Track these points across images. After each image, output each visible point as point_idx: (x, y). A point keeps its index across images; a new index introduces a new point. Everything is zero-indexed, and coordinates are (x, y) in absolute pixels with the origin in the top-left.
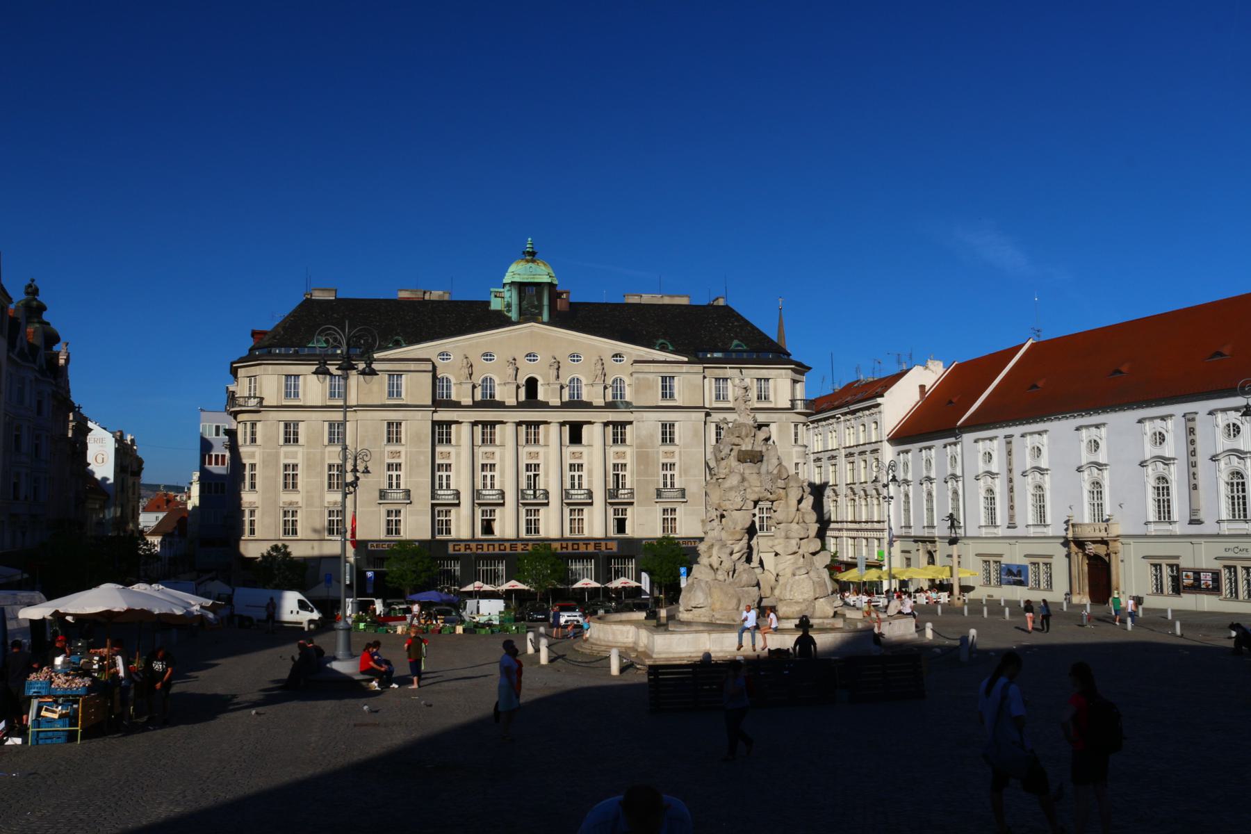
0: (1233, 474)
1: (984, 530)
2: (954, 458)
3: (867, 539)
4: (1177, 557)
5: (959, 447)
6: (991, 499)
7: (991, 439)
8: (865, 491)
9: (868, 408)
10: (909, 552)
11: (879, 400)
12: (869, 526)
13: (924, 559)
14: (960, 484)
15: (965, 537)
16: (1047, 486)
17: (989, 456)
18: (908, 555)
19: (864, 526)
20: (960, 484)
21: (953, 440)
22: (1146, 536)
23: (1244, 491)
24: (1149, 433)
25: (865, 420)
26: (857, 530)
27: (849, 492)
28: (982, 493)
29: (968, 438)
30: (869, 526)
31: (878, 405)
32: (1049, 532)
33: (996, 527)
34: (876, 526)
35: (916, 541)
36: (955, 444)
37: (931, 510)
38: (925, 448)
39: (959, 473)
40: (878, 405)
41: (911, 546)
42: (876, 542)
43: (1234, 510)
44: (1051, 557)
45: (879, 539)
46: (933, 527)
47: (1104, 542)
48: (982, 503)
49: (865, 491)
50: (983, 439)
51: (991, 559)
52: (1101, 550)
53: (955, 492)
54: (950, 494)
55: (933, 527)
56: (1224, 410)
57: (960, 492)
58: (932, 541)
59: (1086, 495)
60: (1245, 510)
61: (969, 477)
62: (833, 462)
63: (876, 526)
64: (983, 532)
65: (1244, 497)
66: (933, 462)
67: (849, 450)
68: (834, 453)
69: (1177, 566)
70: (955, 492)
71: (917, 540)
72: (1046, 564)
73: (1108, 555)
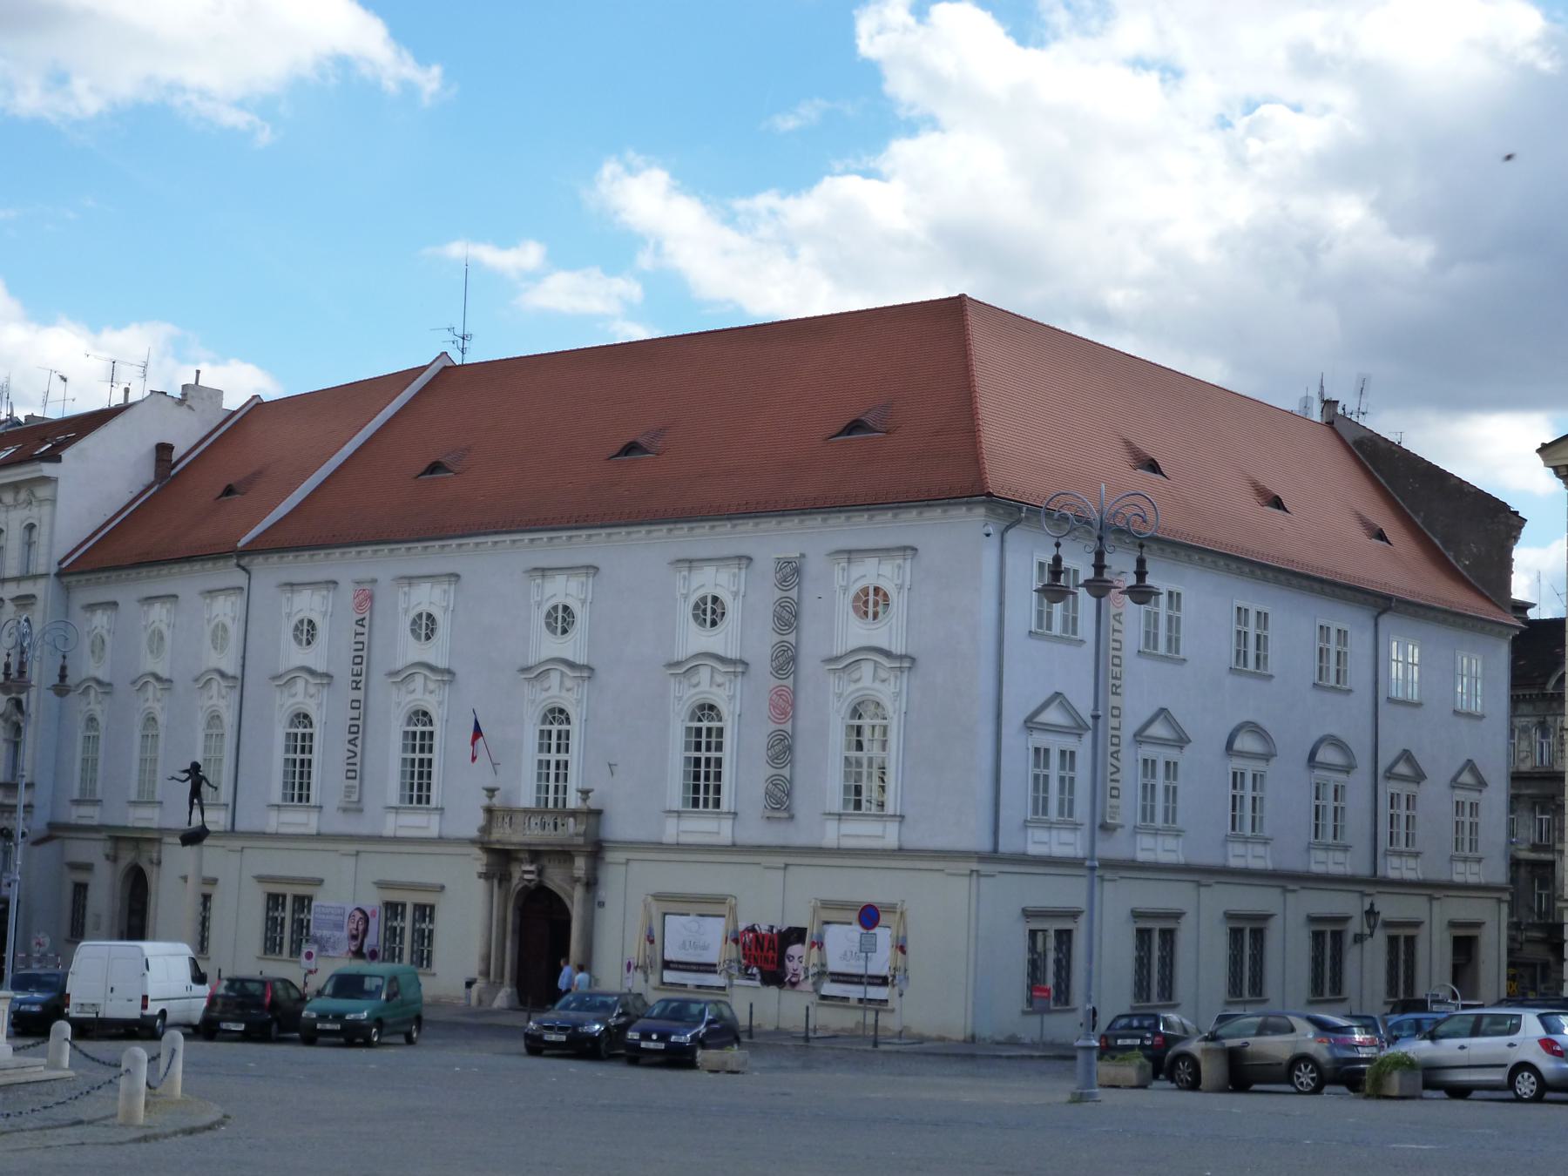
6: (301, 743)
15: (232, 832)
17: (307, 632)
52: (555, 878)
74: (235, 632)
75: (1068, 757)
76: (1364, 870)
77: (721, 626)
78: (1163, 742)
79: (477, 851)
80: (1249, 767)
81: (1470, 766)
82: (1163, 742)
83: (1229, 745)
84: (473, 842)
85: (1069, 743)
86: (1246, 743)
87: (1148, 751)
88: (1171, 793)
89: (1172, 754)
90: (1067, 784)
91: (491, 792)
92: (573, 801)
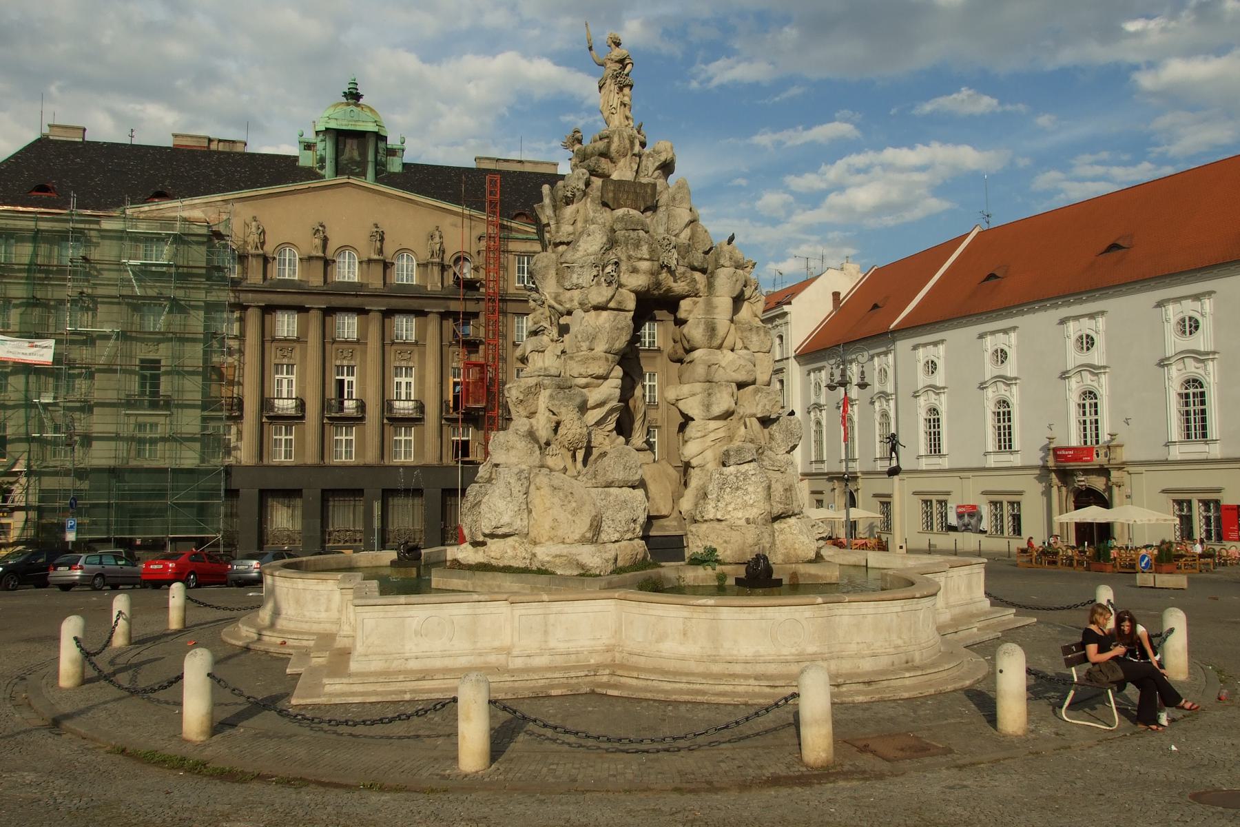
1: (924, 460)
2: (883, 372)
4: (1219, 491)
5: (891, 357)
7: (935, 344)
10: (821, 493)
11: (786, 308)
13: (841, 500)
14: (892, 403)
16: (1015, 401)
18: (819, 497)
20: (892, 403)
21: (884, 349)
22: (1166, 462)
28: (923, 415)
29: (903, 346)
31: (785, 314)
32: (1016, 460)
33: (941, 456)
35: (831, 479)
36: (886, 354)
39: (890, 389)
40: (785, 314)
44: (1020, 493)
47: (1104, 471)
48: (922, 427)
50: (925, 345)
51: (934, 498)
53: (885, 415)
54: (877, 417)
57: (892, 414)
58: (853, 478)
59: (1074, 411)
61: (904, 394)
69: (1217, 502)
70: (885, 415)
71: (832, 477)
73: (1109, 489)
74: (891, 372)
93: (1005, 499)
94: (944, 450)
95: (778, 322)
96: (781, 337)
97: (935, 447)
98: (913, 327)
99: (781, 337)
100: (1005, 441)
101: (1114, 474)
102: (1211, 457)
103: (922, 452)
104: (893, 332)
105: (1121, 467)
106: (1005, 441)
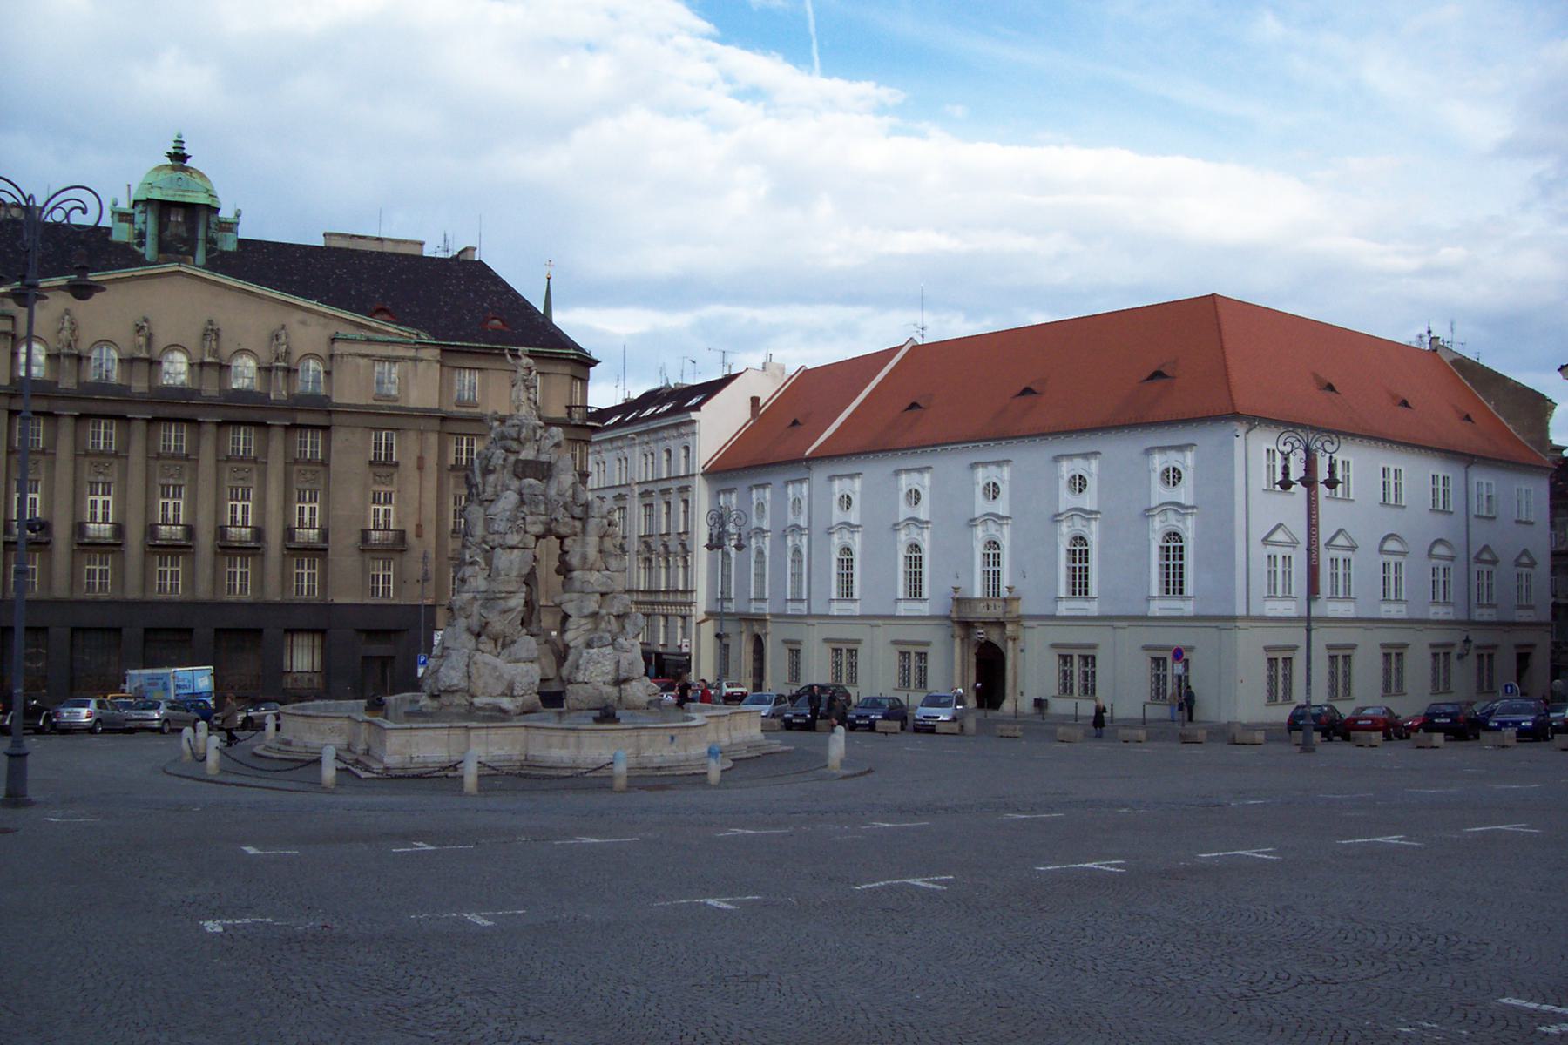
0: (1169, 535)
1: (835, 605)
2: (797, 502)
3: (666, 617)
7: (851, 476)
8: (666, 547)
9: (677, 426)
12: (671, 598)
19: (662, 598)
20: (805, 539)
22: (1053, 617)
23: (1181, 558)
24: (1067, 477)
25: (672, 444)
26: (652, 603)
27: (642, 547)
29: (819, 474)
30: (671, 598)
34: (680, 598)
37: (760, 576)
38: (757, 486)
39: (803, 524)
41: (729, 628)
42: (680, 623)
43: (1167, 583)
45: (684, 617)
46: (763, 600)
47: (1000, 624)
49: (666, 547)
51: (844, 647)
52: (994, 636)
53: (797, 551)
55: (763, 600)
56: (1163, 449)
57: (804, 551)
58: (760, 619)
60: (1181, 583)
62: (621, 504)
63: (680, 598)
64: (835, 609)
65: (1181, 567)
66: (767, 507)
67: (644, 488)
68: (623, 491)
72: (919, 654)
75: (1287, 559)
76: (1463, 616)
77: (1085, 492)
78: (1342, 548)
79: (948, 622)
80: (1392, 560)
81: (1525, 552)
82: (1342, 548)
83: (1381, 546)
84: (948, 617)
85: (1287, 551)
86: (1391, 545)
87: (1334, 553)
88: (1347, 577)
89: (1348, 554)
90: (1288, 575)
91: (956, 589)
92: (1004, 593)
93: (913, 649)
94: (856, 595)
95: (683, 430)
96: (687, 448)
97: (847, 593)
98: (831, 455)
99: (687, 448)
100: (915, 590)
101: (1009, 628)
102: (1089, 614)
103: (834, 596)
104: (808, 459)
105: (1018, 620)
106: (915, 590)
